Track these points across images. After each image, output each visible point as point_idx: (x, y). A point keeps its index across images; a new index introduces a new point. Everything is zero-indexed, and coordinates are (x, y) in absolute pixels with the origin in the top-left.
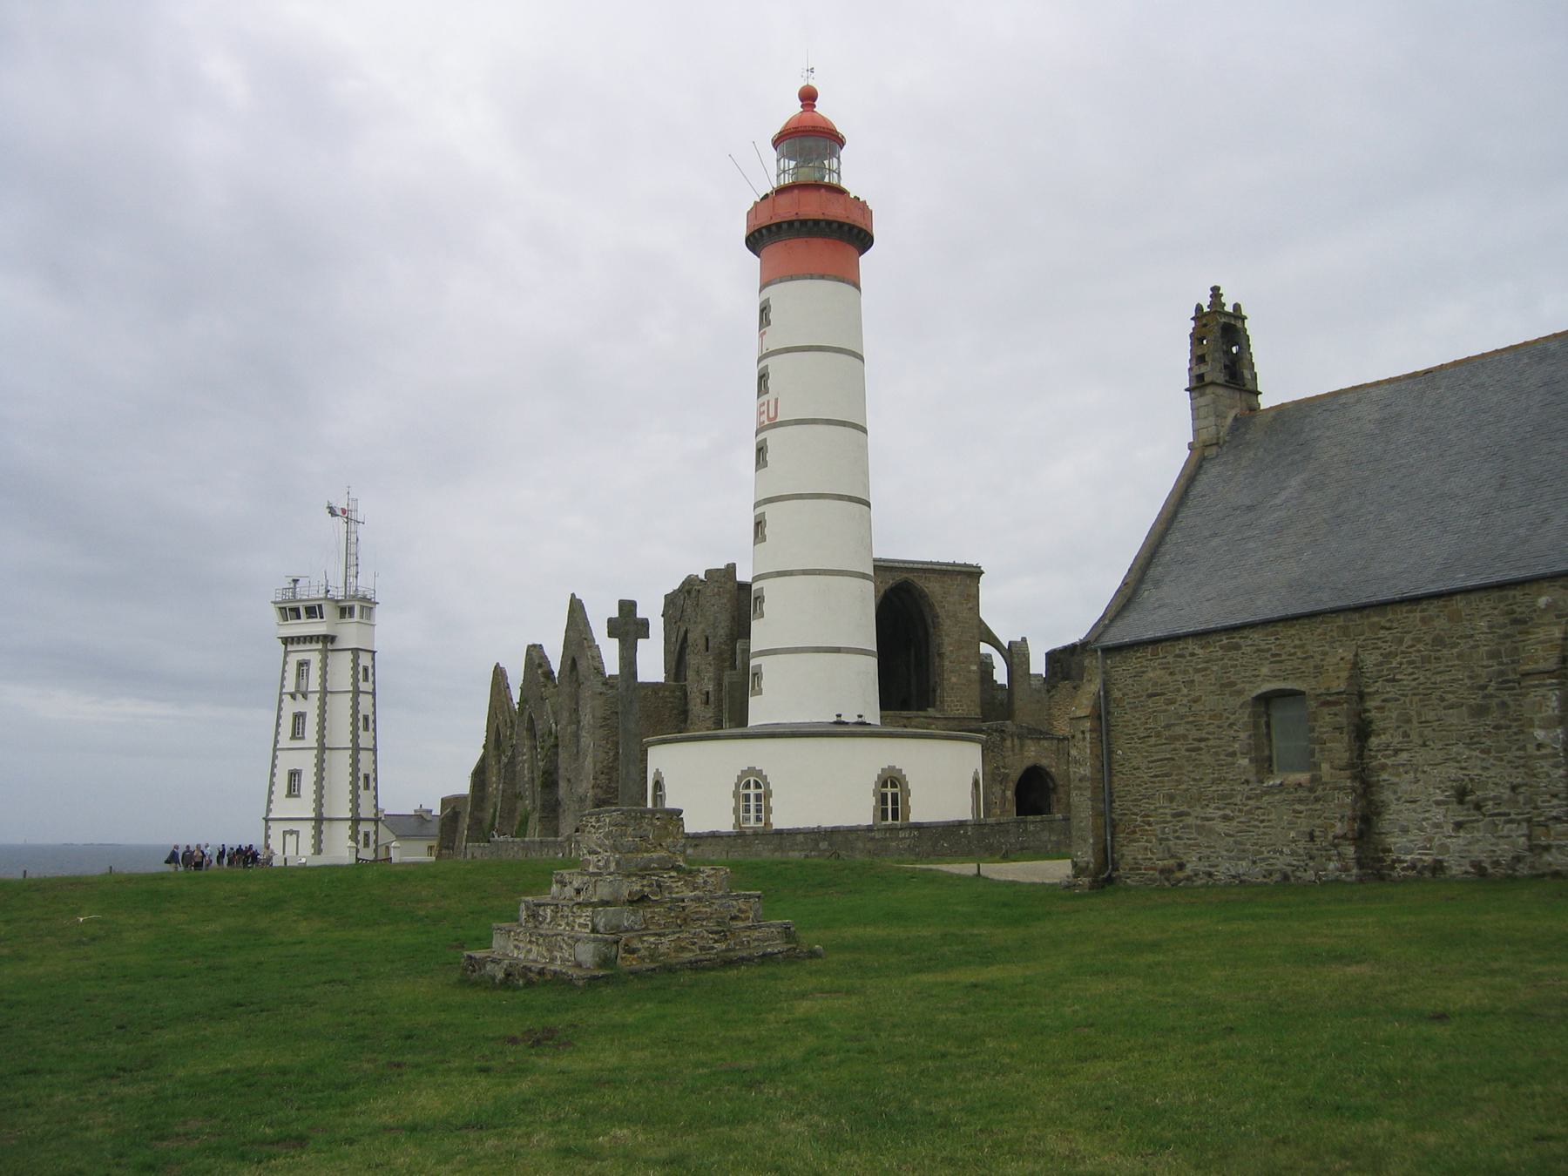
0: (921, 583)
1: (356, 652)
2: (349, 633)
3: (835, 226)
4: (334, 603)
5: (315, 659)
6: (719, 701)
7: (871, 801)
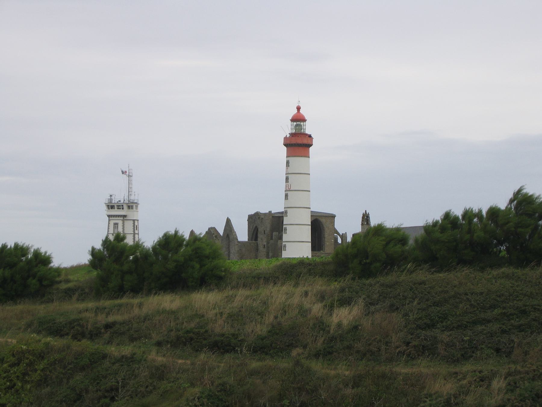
0: (320, 219)
1: (134, 221)
2: (131, 214)
3: (305, 145)
4: (126, 204)
5: (120, 223)
6: (268, 247)
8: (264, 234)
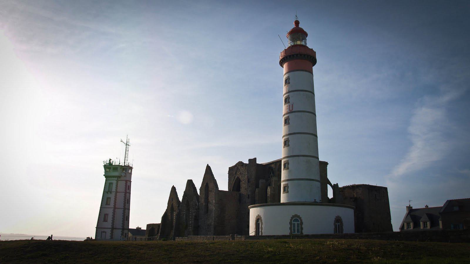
5: (114, 182)
7: (333, 227)
8: (249, 182)
